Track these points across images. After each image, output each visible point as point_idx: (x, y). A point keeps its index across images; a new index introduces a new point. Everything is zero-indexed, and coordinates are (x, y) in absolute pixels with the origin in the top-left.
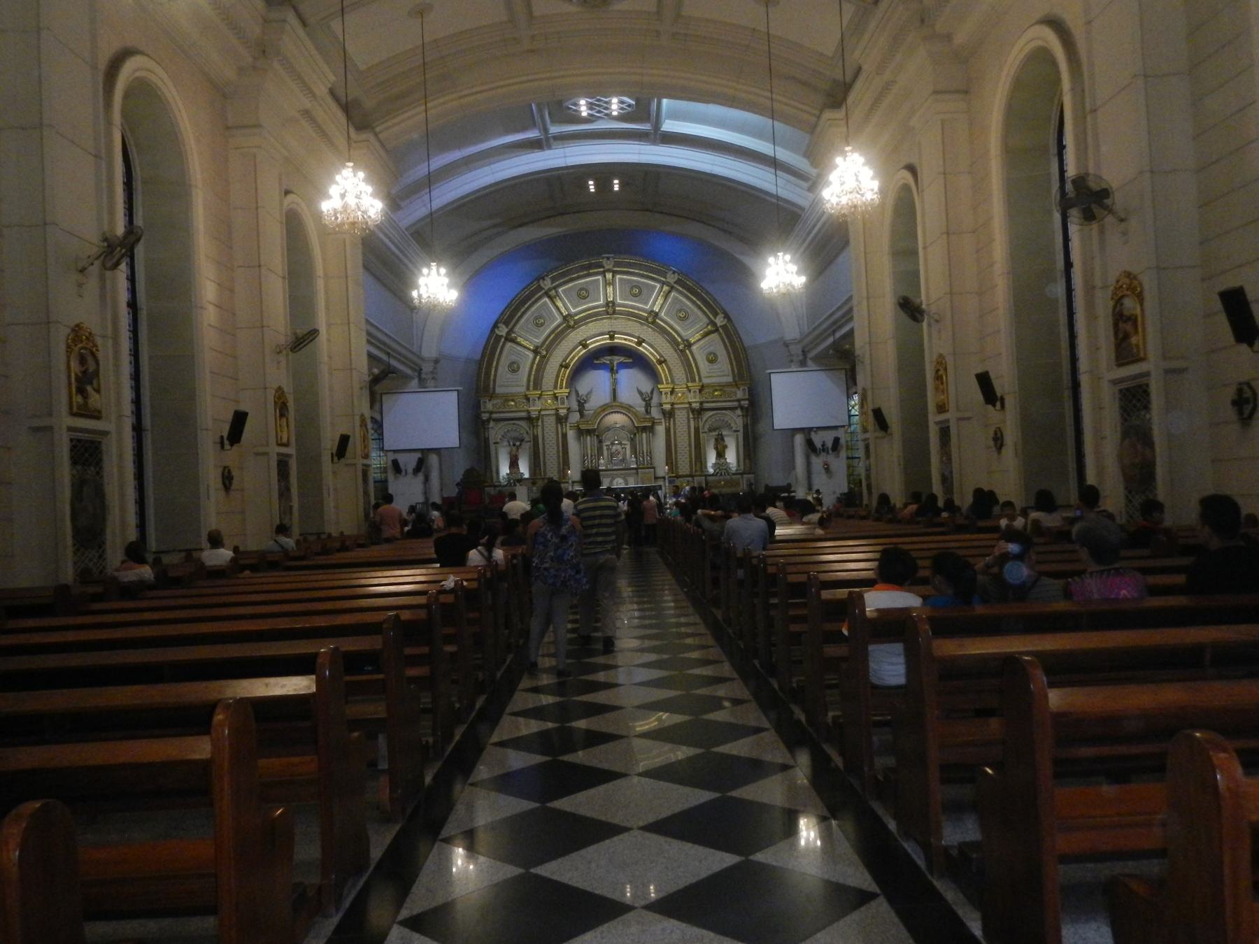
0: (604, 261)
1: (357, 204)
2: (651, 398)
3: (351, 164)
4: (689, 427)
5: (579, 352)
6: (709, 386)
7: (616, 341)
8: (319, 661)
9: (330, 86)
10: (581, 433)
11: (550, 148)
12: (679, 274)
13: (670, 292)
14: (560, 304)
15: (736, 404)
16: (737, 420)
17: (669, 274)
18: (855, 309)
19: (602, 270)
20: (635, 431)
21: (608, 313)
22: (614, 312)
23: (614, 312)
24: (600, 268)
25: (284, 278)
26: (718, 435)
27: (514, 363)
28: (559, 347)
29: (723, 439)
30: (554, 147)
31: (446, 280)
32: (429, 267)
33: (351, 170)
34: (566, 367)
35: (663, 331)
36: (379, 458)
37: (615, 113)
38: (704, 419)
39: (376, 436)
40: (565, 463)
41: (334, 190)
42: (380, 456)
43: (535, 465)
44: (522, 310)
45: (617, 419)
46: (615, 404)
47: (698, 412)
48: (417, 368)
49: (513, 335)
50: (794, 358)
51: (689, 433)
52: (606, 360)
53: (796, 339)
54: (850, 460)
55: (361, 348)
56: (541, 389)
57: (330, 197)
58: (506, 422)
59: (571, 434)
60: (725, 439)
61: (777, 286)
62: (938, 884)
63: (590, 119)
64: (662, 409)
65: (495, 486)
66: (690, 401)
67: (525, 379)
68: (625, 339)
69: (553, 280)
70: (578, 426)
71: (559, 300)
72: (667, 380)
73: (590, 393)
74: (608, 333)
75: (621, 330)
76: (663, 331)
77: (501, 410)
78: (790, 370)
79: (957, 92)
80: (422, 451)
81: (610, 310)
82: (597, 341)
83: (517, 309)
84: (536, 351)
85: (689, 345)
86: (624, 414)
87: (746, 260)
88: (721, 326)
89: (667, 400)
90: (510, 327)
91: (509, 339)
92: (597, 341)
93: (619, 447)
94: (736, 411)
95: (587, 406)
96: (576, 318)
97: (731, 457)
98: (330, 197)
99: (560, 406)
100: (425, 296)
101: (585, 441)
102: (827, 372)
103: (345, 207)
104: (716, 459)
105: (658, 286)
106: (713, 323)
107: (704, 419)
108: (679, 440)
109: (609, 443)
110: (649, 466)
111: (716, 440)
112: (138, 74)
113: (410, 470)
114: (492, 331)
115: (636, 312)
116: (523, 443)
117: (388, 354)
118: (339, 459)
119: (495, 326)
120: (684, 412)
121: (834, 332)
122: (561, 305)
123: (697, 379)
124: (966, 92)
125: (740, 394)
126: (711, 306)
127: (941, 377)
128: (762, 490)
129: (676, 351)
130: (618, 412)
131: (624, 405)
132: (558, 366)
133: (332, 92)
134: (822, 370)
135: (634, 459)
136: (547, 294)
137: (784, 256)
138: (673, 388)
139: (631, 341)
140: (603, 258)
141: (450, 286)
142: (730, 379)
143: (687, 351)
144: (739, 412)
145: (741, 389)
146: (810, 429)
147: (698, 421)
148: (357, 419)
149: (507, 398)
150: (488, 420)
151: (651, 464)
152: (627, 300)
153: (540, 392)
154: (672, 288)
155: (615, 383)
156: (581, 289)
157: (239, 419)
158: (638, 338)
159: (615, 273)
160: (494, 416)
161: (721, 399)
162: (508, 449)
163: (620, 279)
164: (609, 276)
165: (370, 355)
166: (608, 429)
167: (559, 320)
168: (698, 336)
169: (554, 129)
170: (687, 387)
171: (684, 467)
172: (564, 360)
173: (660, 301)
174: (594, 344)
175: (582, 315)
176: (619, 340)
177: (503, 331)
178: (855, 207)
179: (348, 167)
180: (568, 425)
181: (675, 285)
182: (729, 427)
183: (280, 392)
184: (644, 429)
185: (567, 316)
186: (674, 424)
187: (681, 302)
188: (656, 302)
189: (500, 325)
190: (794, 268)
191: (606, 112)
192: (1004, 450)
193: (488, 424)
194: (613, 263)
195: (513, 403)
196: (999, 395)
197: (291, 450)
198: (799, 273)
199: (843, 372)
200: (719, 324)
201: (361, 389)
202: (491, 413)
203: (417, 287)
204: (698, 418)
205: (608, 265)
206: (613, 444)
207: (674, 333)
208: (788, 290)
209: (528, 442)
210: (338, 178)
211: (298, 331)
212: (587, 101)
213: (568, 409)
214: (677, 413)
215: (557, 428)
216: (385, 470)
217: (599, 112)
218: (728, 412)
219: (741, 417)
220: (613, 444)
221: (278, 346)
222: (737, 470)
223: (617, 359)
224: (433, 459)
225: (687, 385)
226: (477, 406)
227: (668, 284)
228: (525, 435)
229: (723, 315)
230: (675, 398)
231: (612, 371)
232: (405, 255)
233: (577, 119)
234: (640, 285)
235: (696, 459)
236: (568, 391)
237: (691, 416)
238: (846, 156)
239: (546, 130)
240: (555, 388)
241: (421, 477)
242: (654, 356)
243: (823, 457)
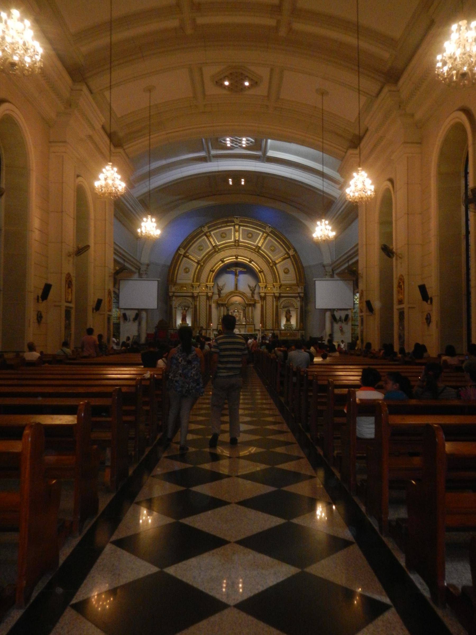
0: (235, 220)
1: (113, 184)
2: (255, 290)
3: (111, 164)
5: (220, 264)
6: (284, 285)
7: (239, 260)
8: (79, 408)
9: (102, 124)
10: (219, 305)
11: (210, 161)
12: (272, 228)
13: (267, 237)
14: (211, 240)
15: (297, 295)
16: (297, 303)
17: (267, 228)
18: (360, 251)
19: (233, 224)
20: (246, 306)
21: (235, 246)
22: (239, 246)
23: (239, 246)
24: (233, 223)
25: (74, 219)
26: (288, 310)
27: (186, 268)
28: (210, 261)
29: (290, 313)
30: (213, 161)
31: (155, 225)
32: (147, 218)
33: (110, 166)
34: (213, 271)
35: (263, 256)
36: (116, 312)
37: (244, 146)
38: (281, 302)
39: (116, 301)
40: (209, 320)
41: (101, 176)
42: (117, 311)
43: (195, 320)
44: (193, 242)
45: (237, 299)
46: (236, 292)
47: (278, 298)
48: (138, 268)
49: (187, 254)
50: (328, 274)
51: (273, 309)
52: (233, 269)
53: (329, 264)
54: (353, 327)
55: (110, 256)
56: (200, 282)
57: (99, 179)
58: (181, 298)
59: (213, 306)
60: (291, 312)
61: (321, 237)
62: (385, 539)
63: (231, 148)
64: (260, 296)
65: (174, 330)
66: (275, 292)
67: (192, 277)
68: (243, 259)
69: (209, 227)
70: (217, 302)
71: (211, 238)
72: (263, 281)
73: (224, 286)
74: (235, 256)
75: (242, 254)
76: (263, 256)
77: (179, 291)
78: (324, 279)
79: (417, 143)
80: (138, 309)
81: (237, 244)
82: (229, 259)
83: (190, 241)
84: (198, 263)
85: (275, 264)
86: (241, 297)
87: (306, 223)
88: (292, 255)
89: (262, 291)
90: (186, 250)
91: (184, 256)
92: (229, 259)
93: (237, 313)
95: (222, 292)
96: (219, 247)
97: (293, 322)
98: (99, 179)
99: (209, 291)
100: (144, 232)
101: (220, 310)
103: (107, 185)
104: (286, 322)
105: (261, 233)
106: (288, 253)
107: (281, 302)
108: (268, 311)
109: (232, 311)
110: (252, 324)
111: (286, 313)
112: (7, 112)
113: (132, 319)
114: (177, 251)
115: (250, 246)
116: (189, 309)
117: (124, 260)
118: (96, 311)
119: (179, 249)
120: (271, 298)
121: (348, 261)
122: (212, 240)
123: (278, 280)
124: (420, 143)
125: (299, 290)
126: (287, 245)
127: (401, 286)
128: (308, 339)
129: (268, 266)
130: (238, 296)
131: (241, 293)
132: (209, 271)
133: (103, 128)
135: (245, 320)
136: (205, 235)
137: (325, 221)
138: (266, 285)
139: (246, 260)
140: (234, 218)
141: (157, 228)
142: (295, 282)
143: (274, 267)
144: (299, 299)
145: (300, 287)
146: (334, 310)
147: (278, 303)
148: (107, 291)
149: (182, 286)
150: (172, 296)
151: (253, 323)
152: (246, 240)
153: (199, 284)
154: (268, 235)
155: (237, 281)
156: (223, 233)
157: (48, 288)
158: (250, 259)
159: (240, 226)
160: (176, 294)
161: (291, 292)
162: (182, 311)
163: (242, 229)
164: (237, 227)
165: (115, 260)
166: (232, 304)
167: (211, 248)
168: (280, 260)
169: (213, 152)
170: (273, 285)
171: (269, 325)
172: (212, 268)
173: (262, 241)
174: (227, 261)
175: (222, 246)
176: (240, 259)
177: (182, 252)
178: (362, 198)
179: (109, 165)
180: (212, 301)
181: (270, 234)
183: (69, 275)
184: (250, 305)
185: (215, 246)
186: (266, 303)
187: (273, 242)
188: (260, 241)
189: (181, 249)
190: (329, 228)
191: (240, 145)
192: (431, 325)
193: (172, 298)
194: (239, 221)
195: (185, 288)
196: (430, 296)
197: (72, 305)
198: (332, 230)
200: (291, 254)
201: (110, 276)
202: (174, 292)
203: (140, 227)
204: (278, 301)
205: (237, 221)
206: (234, 312)
207: (268, 258)
208: (326, 238)
209: (191, 308)
210: (104, 170)
211: (80, 246)
212: (230, 139)
213: (213, 293)
214: (267, 298)
215: (207, 302)
216: (119, 318)
217: (236, 144)
219: (300, 302)
220: (234, 312)
221: (69, 252)
222: (296, 328)
223: (239, 269)
224: (144, 314)
225: (273, 284)
226: (168, 289)
227: (266, 233)
228: (190, 305)
229: (293, 250)
230: (267, 291)
231: (236, 275)
232: (135, 210)
233: (225, 147)
234: (251, 232)
235: (276, 321)
236: (213, 284)
237: (274, 300)
238: (359, 172)
239: (209, 152)
240: (207, 282)
241: (136, 323)
242: (257, 269)
243: (340, 323)
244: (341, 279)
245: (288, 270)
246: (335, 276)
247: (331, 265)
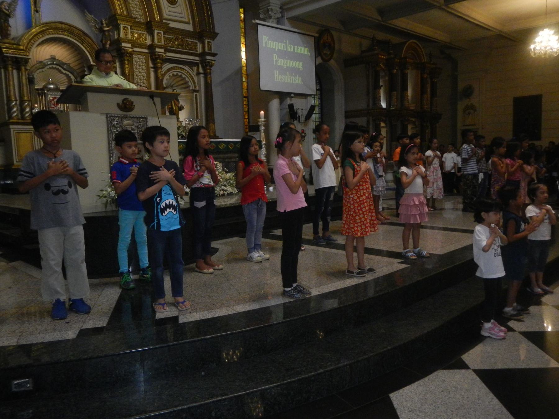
94: (195, 68)
102: (301, 36)
120: (142, 58)
145: (206, 41)
199: (313, 38)
237: (151, 65)
246: (286, 22)
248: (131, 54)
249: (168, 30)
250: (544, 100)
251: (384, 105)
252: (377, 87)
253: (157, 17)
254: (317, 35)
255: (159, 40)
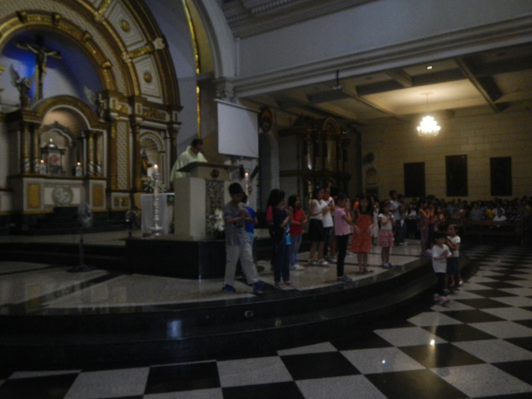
4: (128, 142)
15: (164, 126)
94: (163, 134)
120: (124, 124)
134: (248, 110)
145: (174, 112)
182: (154, 147)
218: (156, 133)
237: (130, 130)
244: (247, 108)
245: (151, 76)
246: (238, 101)
247: (235, 81)
248: (117, 121)
249: (146, 103)
250: (426, 166)
251: (310, 167)
252: (305, 153)
253: (137, 93)
254: (260, 111)
255: (139, 111)
